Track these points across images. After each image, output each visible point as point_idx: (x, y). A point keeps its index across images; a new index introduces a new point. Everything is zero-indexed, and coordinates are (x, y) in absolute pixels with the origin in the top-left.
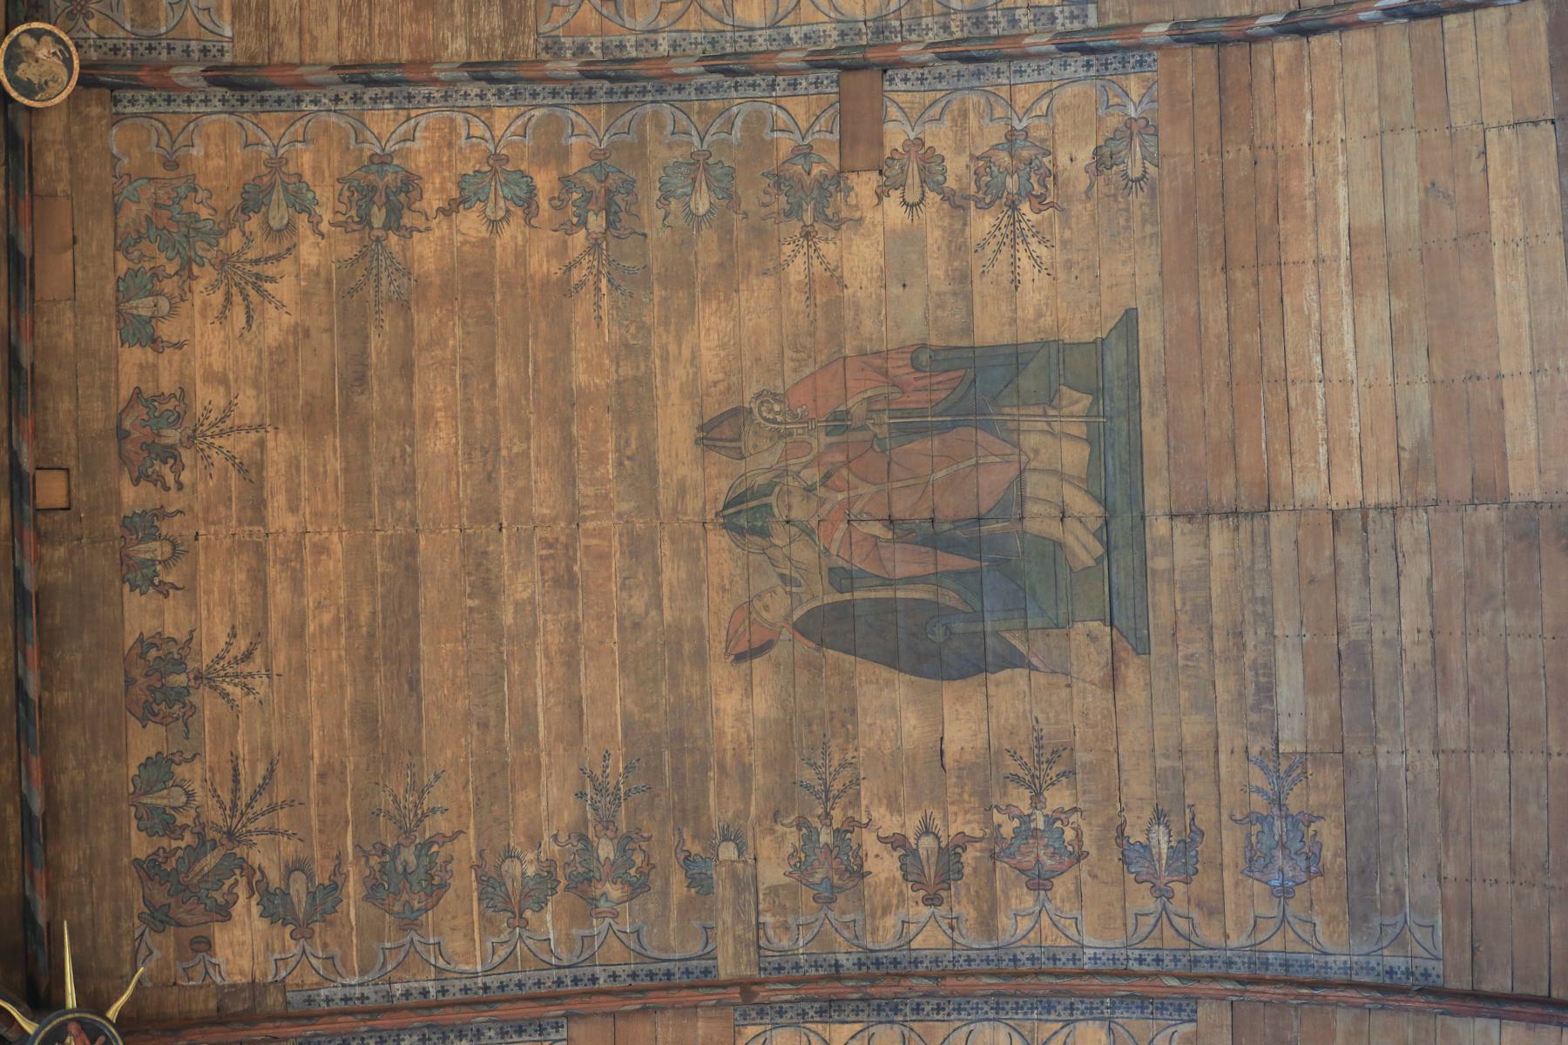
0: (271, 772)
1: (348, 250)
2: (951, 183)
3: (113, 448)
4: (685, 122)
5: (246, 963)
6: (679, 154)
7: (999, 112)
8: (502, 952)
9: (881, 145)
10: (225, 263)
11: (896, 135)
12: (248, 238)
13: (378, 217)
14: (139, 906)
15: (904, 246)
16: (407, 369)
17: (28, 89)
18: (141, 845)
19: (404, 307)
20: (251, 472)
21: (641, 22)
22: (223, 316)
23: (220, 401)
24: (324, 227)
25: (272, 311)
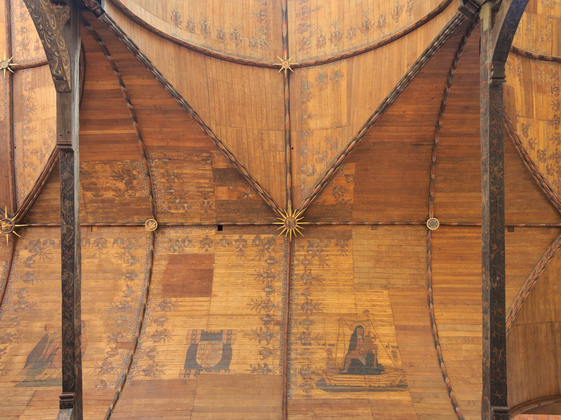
0: (49, 259)
1: (124, 271)
2: (109, 358)
3: (99, 237)
4: (132, 319)
5: (22, 254)
6: (128, 318)
7: (118, 366)
8: (13, 291)
9: (120, 348)
10: (124, 253)
11: (120, 351)
12: (127, 257)
13: (128, 275)
14: (33, 239)
15: (101, 351)
16: (104, 279)
17: (148, 223)
18: (42, 240)
19: (114, 279)
20: (93, 257)
21: (151, 313)
22: (117, 253)
23: (104, 252)
24: (128, 267)
25: (116, 260)
